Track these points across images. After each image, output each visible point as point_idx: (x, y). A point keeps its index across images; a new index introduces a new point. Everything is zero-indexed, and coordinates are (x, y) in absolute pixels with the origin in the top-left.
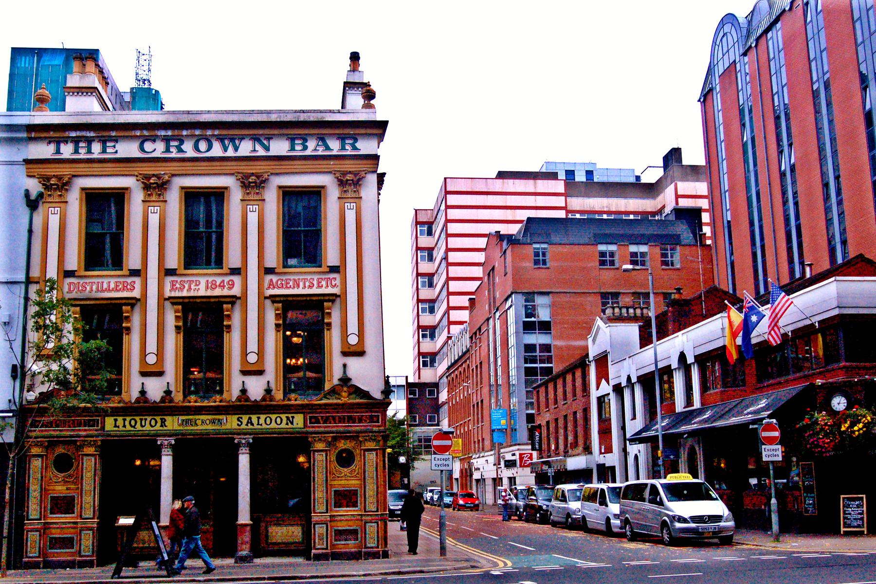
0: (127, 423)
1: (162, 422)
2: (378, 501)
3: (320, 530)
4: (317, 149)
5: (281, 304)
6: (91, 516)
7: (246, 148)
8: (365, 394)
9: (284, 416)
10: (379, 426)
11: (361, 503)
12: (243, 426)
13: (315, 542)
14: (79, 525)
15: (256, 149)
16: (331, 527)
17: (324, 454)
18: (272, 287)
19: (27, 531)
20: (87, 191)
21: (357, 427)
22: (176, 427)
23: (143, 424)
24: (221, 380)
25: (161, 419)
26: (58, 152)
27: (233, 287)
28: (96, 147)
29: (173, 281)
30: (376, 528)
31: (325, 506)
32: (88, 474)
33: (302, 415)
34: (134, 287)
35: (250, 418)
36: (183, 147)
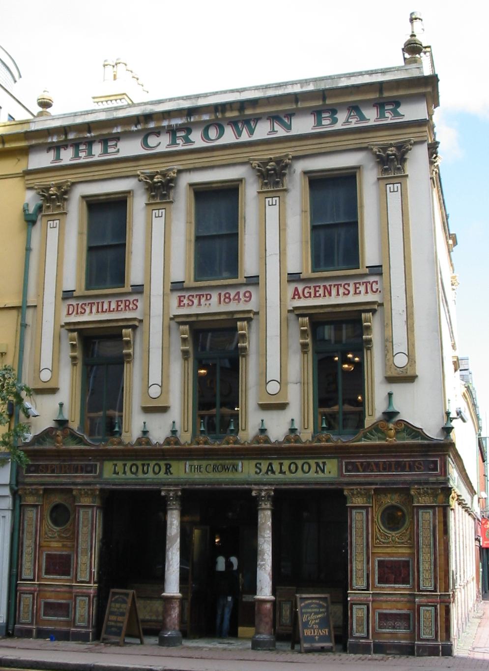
0: (127, 469)
1: (167, 469)
2: (435, 578)
3: (358, 613)
4: (350, 120)
5: (307, 318)
6: (87, 579)
7: (262, 131)
8: (416, 432)
9: (312, 462)
10: (436, 475)
11: (414, 579)
13: (352, 628)
14: (75, 590)
15: (275, 130)
16: (374, 610)
17: (364, 512)
18: (296, 297)
19: (20, 594)
20: (88, 199)
21: (407, 476)
22: (182, 475)
24: (236, 416)
25: (166, 465)
26: (58, 158)
27: (250, 299)
28: (97, 149)
29: (180, 297)
30: (433, 614)
31: (365, 581)
32: (85, 529)
33: (335, 461)
34: (137, 307)
35: (270, 464)
36: (191, 137)
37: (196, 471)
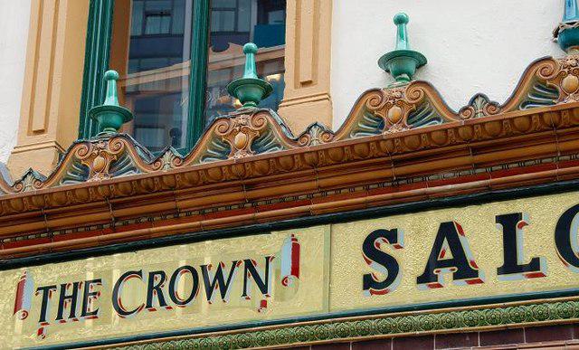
12: (406, 291)
35: (449, 232)
37: (67, 312)
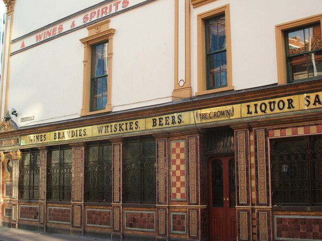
1: (289, 103)
23: (272, 108)
25: (288, 100)
35: (317, 96)
